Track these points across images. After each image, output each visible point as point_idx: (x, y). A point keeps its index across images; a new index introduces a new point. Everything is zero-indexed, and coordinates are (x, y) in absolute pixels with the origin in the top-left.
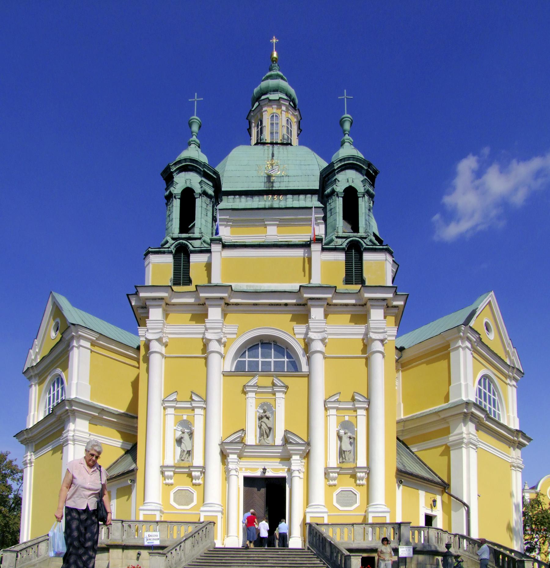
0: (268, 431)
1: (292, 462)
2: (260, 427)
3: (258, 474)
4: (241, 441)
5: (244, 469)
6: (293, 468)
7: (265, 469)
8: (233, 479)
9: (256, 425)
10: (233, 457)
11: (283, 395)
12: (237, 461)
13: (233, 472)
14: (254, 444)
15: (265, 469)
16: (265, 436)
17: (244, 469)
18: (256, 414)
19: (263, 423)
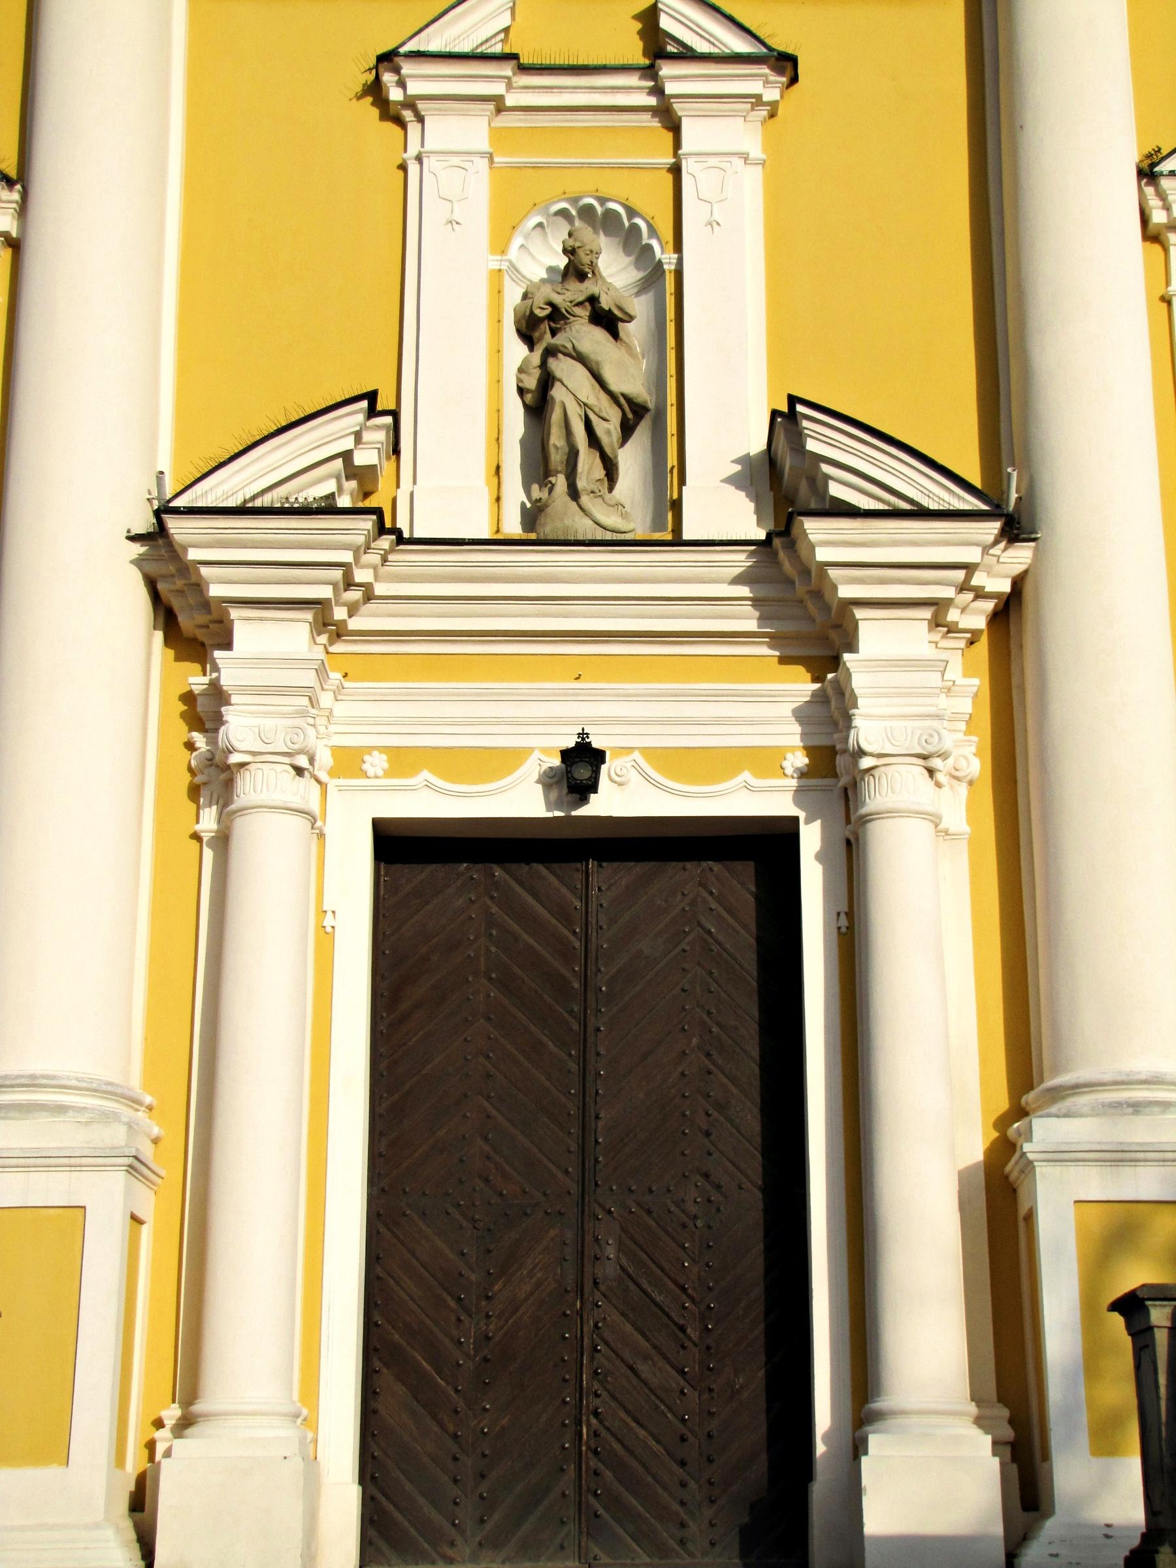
0: (608, 430)
1: (860, 682)
2: (538, 406)
3: (522, 799)
4: (365, 504)
5: (376, 763)
6: (869, 730)
7: (580, 766)
8: (270, 849)
9: (497, 381)
10: (265, 648)
11: (744, 134)
12: (308, 678)
13: (260, 786)
14: (486, 535)
15: (580, 766)
16: (589, 466)
17: (376, 763)
18: (498, 293)
19: (562, 367)
